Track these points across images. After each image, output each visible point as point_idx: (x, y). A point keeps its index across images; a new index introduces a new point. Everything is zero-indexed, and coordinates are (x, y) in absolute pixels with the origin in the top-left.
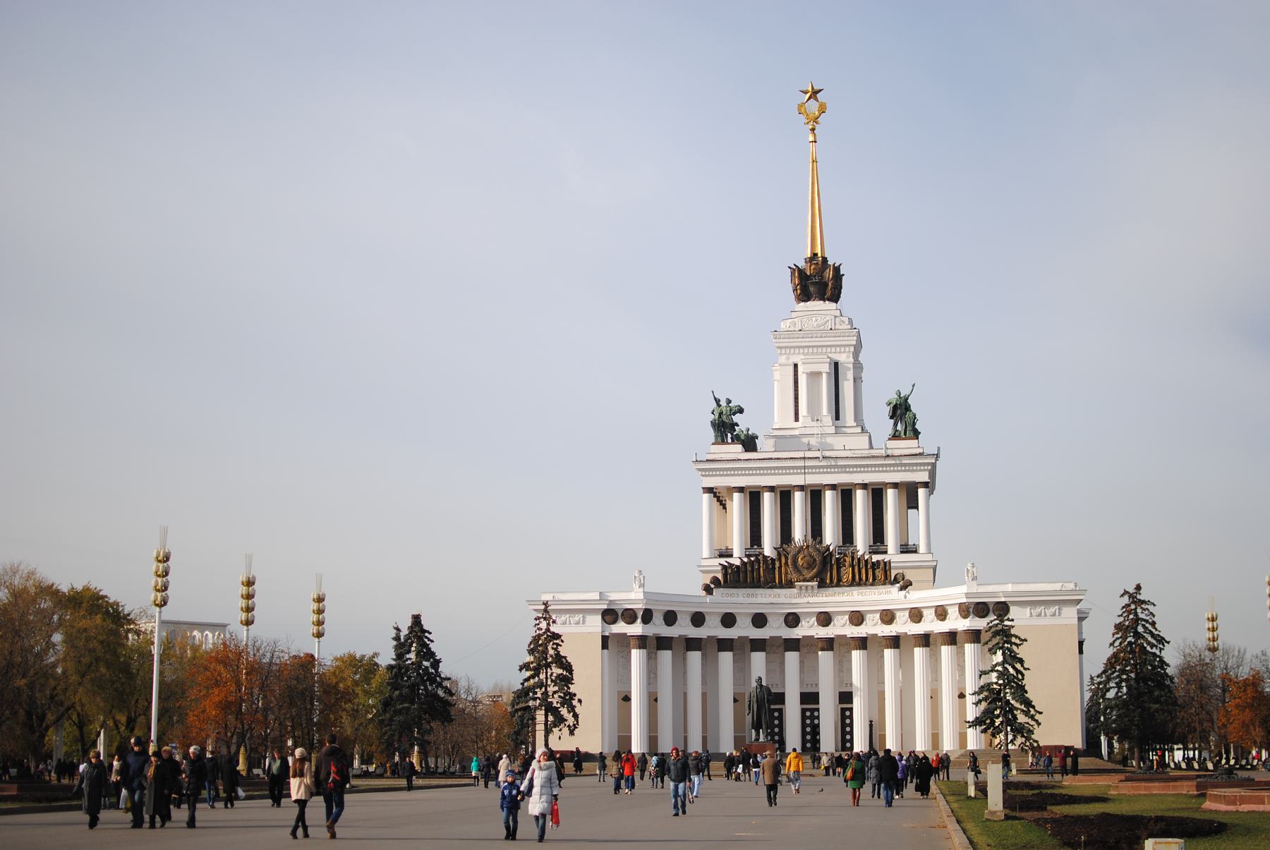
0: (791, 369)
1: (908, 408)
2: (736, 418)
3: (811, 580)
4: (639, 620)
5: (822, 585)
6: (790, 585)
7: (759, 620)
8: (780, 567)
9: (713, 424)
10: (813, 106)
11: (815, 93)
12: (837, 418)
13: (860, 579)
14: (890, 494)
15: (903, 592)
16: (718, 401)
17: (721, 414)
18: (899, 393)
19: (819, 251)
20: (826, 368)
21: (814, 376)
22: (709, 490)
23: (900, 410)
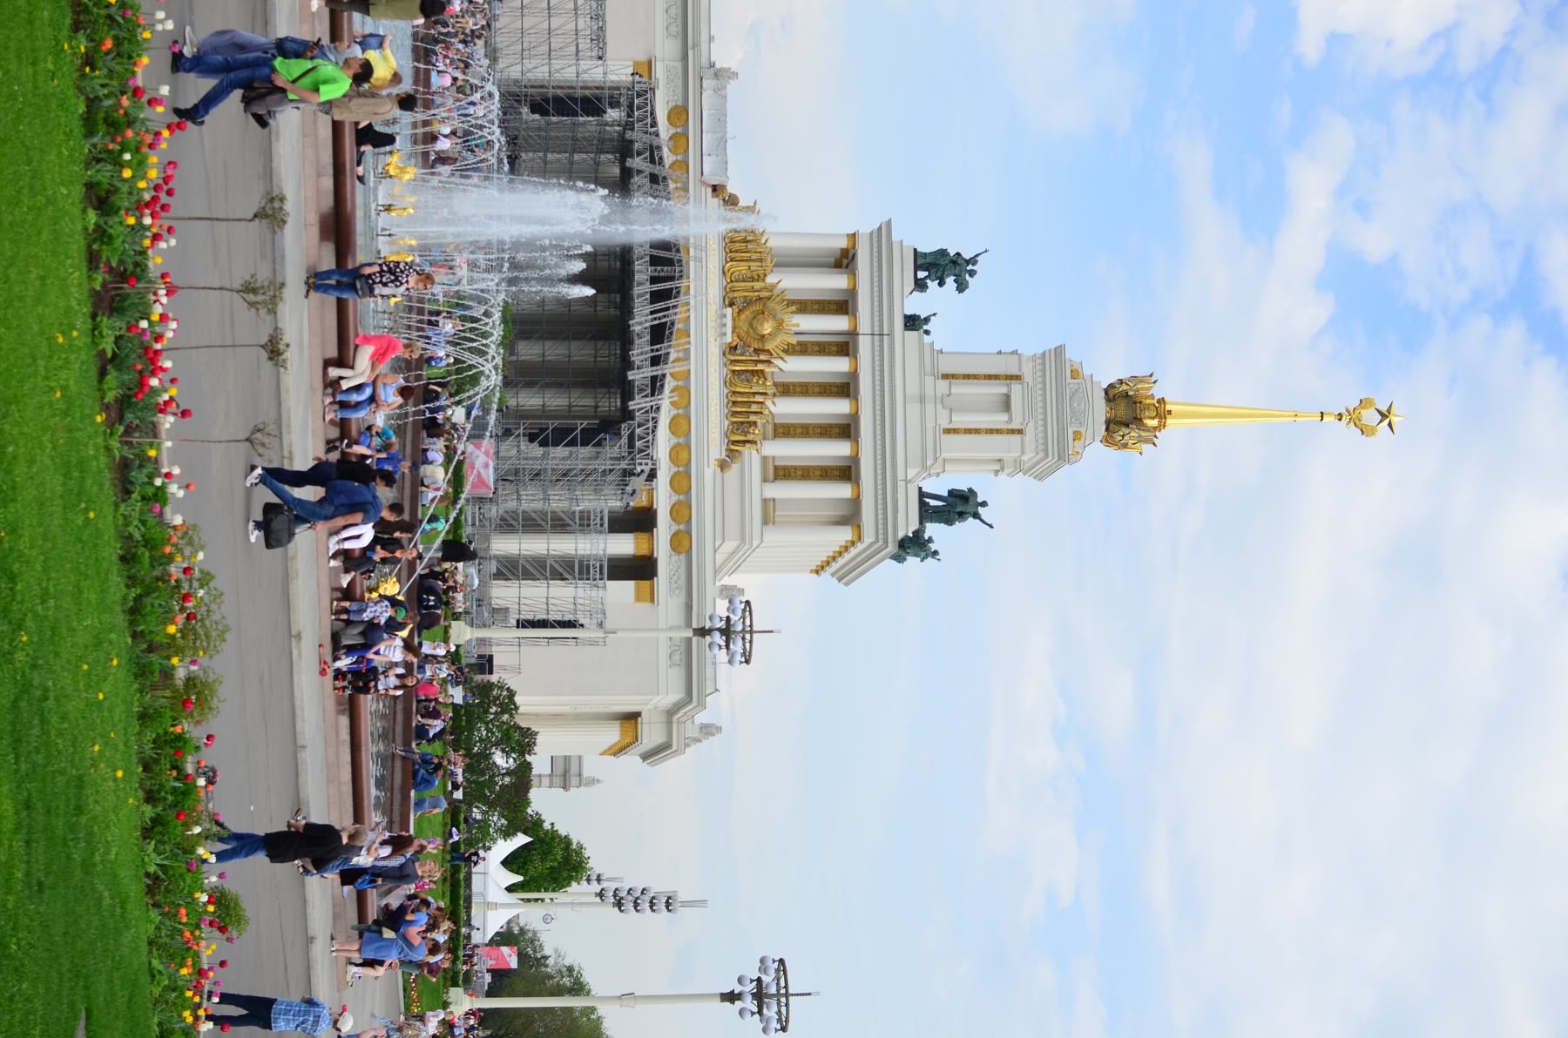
0: (1015, 372)
1: (962, 516)
2: (950, 280)
3: (734, 328)
9: (943, 253)
10: (1370, 417)
12: (947, 431)
16: (973, 261)
17: (954, 262)
18: (984, 504)
21: (1006, 404)
22: (853, 237)
23: (960, 505)
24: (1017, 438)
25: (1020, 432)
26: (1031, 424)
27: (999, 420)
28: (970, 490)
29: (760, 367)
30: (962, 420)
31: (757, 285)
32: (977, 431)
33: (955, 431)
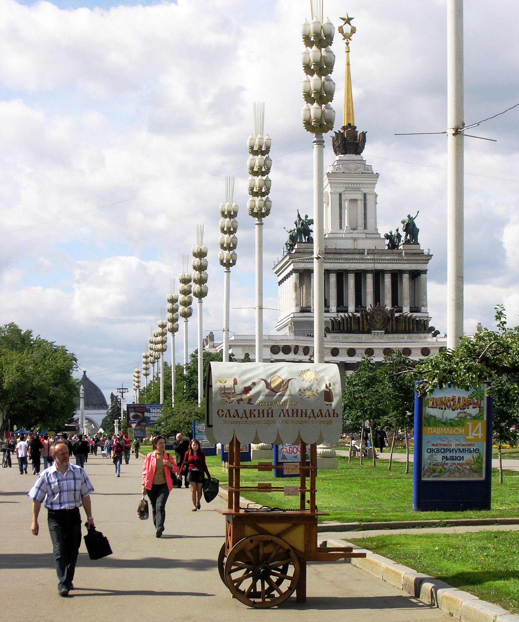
0: (338, 196)
1: (414, 225)
4: (292, 352)
5: (387, 332)
6: (369, 332)
7: (351, 352)
8: (363, 322)
10: (347, 29)
11: (348, 21)
12: (365, 228)
13: (409, 330)
14: (406, 277)
15: (435, 338)
17: (302, 225)
18: (409, 216)
19: (351, 123)
20: (360, 196)
21: (354, 201)
24: (368, 197)
25: (365, 195)
26: (361, 189)
27: (360, 204)
28: (403, 222)
29: (394, 319)
30: (361, 222)
31: (361, 320)
32: (365, 214)
33: (365, 224)
